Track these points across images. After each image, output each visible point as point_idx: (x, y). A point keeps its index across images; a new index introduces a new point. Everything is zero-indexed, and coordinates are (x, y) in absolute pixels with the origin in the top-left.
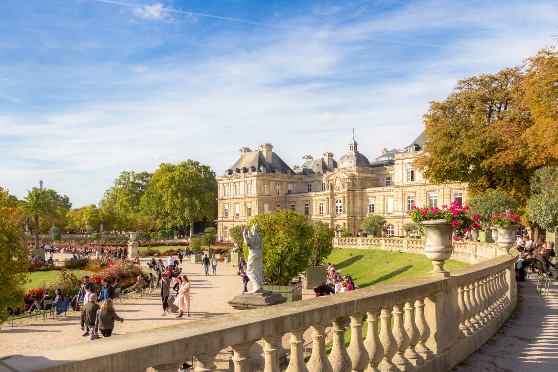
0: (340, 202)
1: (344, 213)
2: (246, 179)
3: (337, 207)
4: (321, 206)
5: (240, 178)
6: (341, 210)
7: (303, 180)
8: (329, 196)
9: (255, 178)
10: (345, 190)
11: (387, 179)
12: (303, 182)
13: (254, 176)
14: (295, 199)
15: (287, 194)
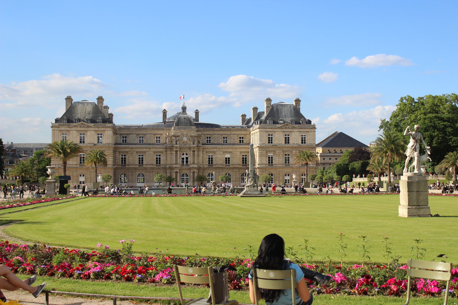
0: (187, 154)
1: (194, 163)
2: (97, 129)
3: (183, 159)
4: (158, 157)
5: (88, 127)
6: (187, 162)
7: (118, 132)
8: (178, 149)
9: (110, 129)
10: (195, 145)
11: (207, 138)
12: (117, 134)
13: (109, 127)
14: (127, 150)
15: (115, 144)
